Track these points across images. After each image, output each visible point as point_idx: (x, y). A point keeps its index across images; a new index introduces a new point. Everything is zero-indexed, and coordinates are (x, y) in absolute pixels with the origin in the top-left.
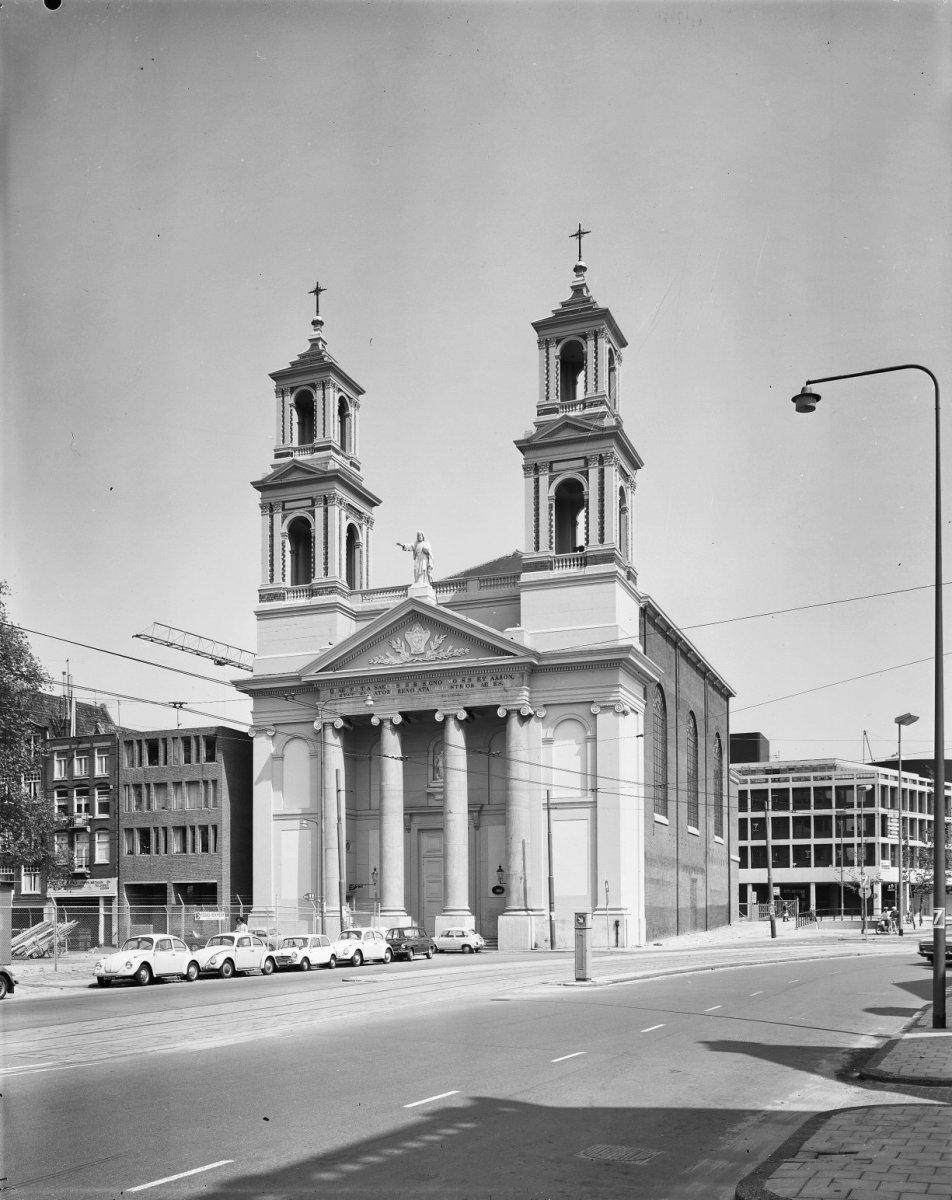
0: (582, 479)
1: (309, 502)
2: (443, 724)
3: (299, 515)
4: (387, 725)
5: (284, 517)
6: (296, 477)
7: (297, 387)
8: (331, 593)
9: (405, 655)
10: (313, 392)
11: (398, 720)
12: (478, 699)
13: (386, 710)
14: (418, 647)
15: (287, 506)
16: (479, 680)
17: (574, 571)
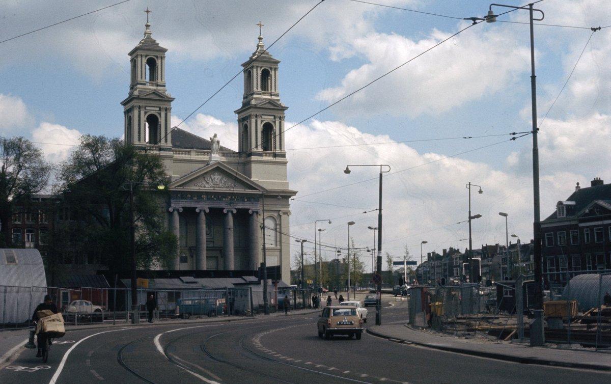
0: (273, 124)
1: (158, 109)
2: (226, 215)
3: (153, 113)
4: (203, 213)
5: (146, 113)
6: (152, 97)
7: (148, 55)
8: (169, 151)
9: (211, 184)
10: (156, 59)
11: (207, 211)
12: (241, 206)
13: (203, 206)
14: (216, 184)
15: (147, 108)
16: (241, 198)
17: (271, 159)
